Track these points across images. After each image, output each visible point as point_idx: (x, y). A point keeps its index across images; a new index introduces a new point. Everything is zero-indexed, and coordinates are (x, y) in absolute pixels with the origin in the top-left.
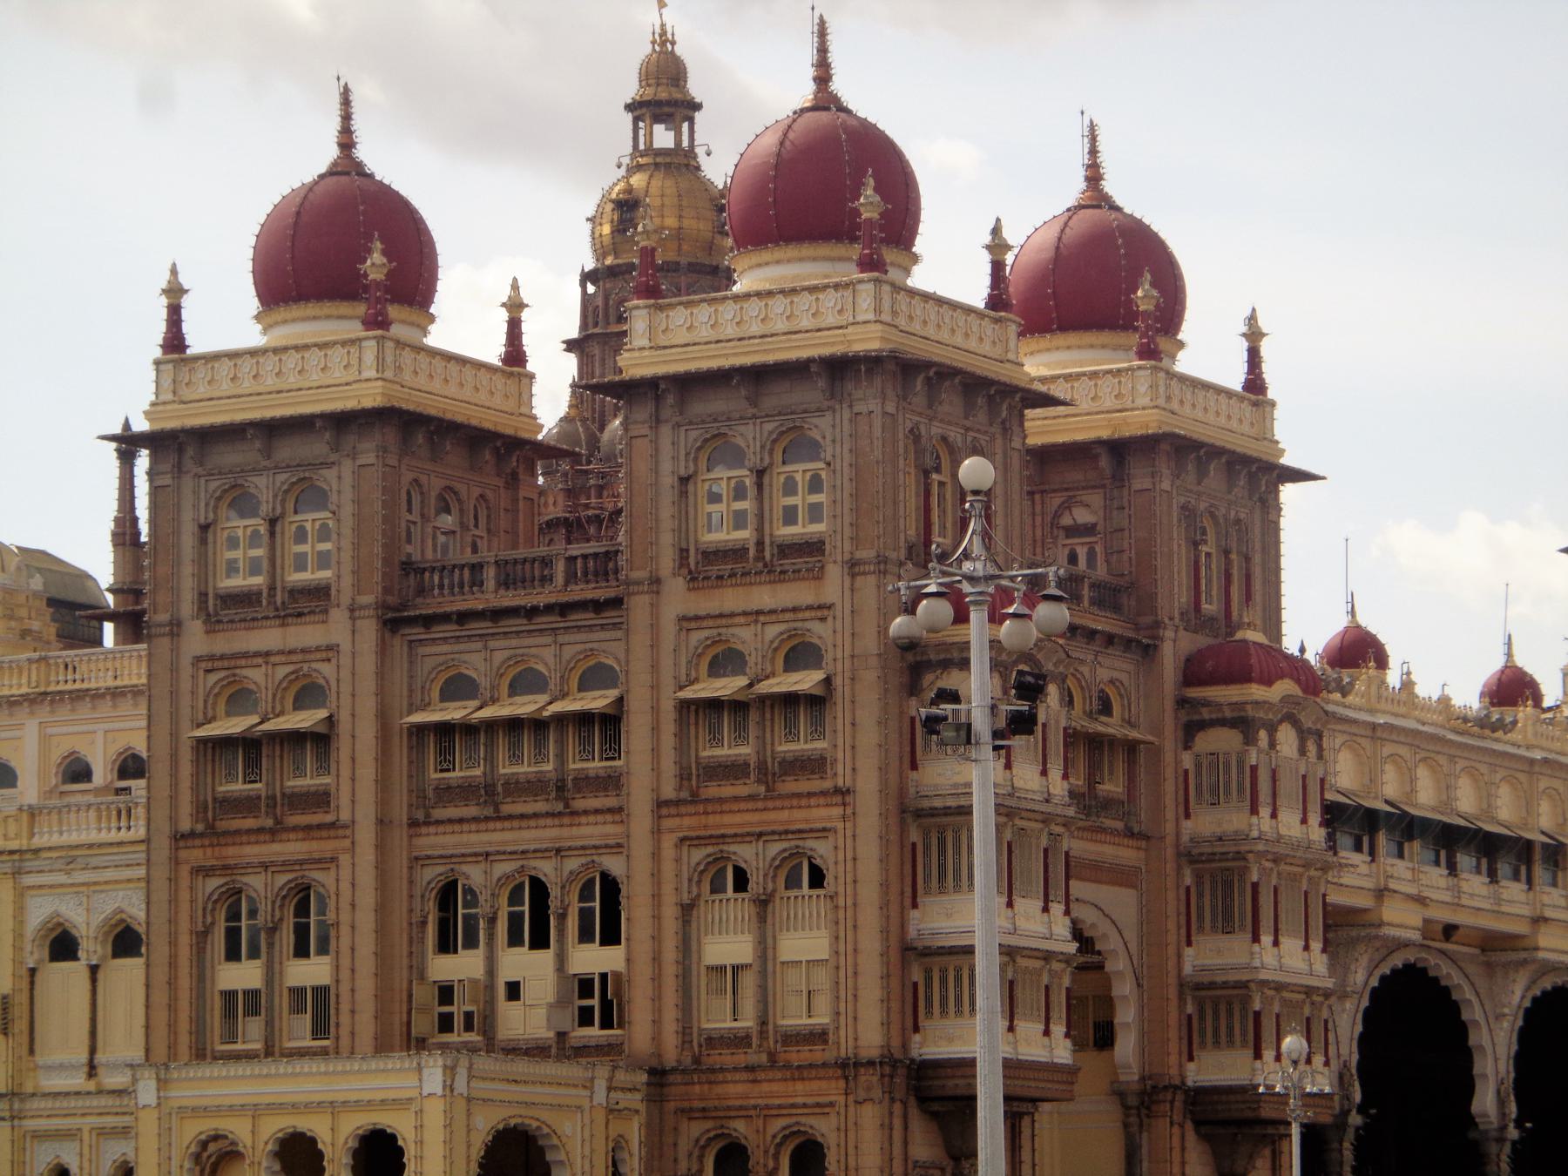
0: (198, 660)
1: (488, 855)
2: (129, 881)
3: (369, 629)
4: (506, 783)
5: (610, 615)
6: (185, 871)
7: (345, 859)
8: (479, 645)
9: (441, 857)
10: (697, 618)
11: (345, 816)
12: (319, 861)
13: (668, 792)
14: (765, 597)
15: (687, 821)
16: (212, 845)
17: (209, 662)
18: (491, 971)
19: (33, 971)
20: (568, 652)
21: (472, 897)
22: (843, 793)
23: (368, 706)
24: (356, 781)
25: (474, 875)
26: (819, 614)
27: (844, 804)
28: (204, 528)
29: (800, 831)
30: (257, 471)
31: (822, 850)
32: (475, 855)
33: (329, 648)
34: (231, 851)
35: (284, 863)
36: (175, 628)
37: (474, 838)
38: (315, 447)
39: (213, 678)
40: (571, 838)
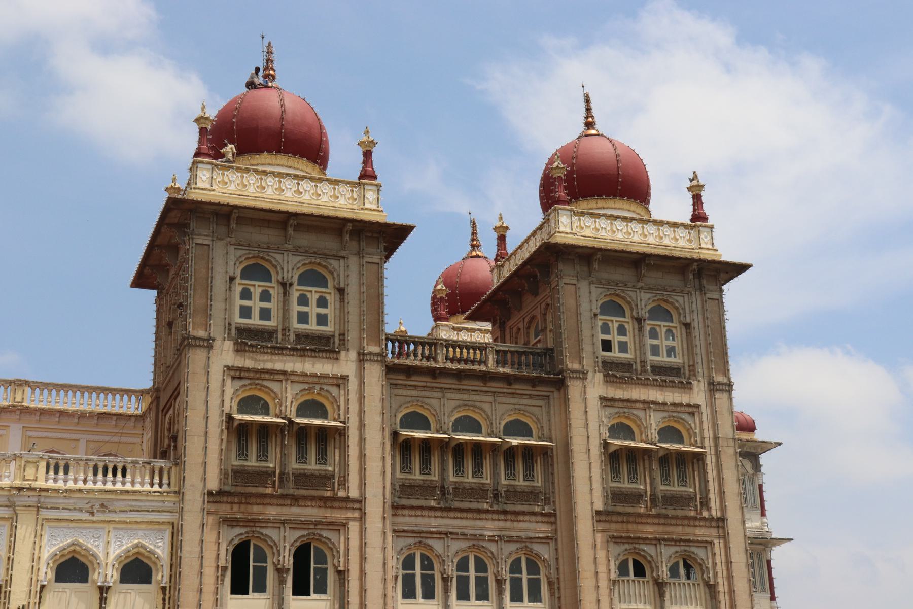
0: (229, 368)
2: (151, 523)
7: (354, 527)
8: (440, 395)
9: (413, 532)
11: (354, 493)
12: (332, 524)
13: (599, 506)
14: (655, 395)
15: (613, 526)
16: (240, 503)
17: (236, 373)
20: (501, 408)
21: (427, 564)
23: (374, 420)
24: (370, 469)
26: (691, 410)
27: (718, 527)
28: (232, 279)
29: (689, 541)
31: (700, 553)
32: (440, 533)
34: (255, 509)
35: (302, 523)
36: (208, 343)
38: (328, 243)
40: (514, 529)
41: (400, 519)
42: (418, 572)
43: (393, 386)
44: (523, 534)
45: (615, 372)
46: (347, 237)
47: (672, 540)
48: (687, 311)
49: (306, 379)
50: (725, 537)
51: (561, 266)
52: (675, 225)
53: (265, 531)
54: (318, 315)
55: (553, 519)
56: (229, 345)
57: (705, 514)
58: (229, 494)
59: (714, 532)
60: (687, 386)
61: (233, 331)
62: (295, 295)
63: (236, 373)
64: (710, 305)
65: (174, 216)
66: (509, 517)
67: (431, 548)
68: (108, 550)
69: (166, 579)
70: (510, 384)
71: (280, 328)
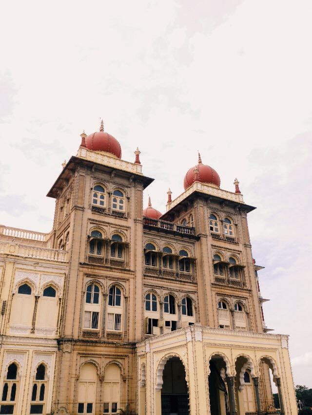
0: (90, 219)
1: (165, 287)
2: (57, 273)
3: (140, 227)
4: (164, 271)
5: (192, 241)
6: (81, 274)
9: (151, 285)
10: (215, 246)
11: (132, 269)
12: (124, 279)
17: (92, 221)
18: (162, 317)
19: (13, 294)
22: (250, 291)
25: (158, 291)
30: (108, 182)
31: (244, 302)
32: (159, 287)
33: (129, 228)
34: (97, 271)
35: (113, 278)
36: (83, 209)
37: (159, 282)
39: (92, 225)
41: (146, 280)
42: (151, 301)
43: (145, 233)
44: (187, 290)
45: (216, 237)
46: (131, 180)
47: (235, 296)
48: (236, 220)
49: (116, 227)
50: (252, 296)
51: (198, 201)
52: (232, 193)
53: (99, 280)
54: (120, 206)
55: (196, 285)
56: (90, 211)
57: (245, 288)
58: (88, 265)
59: (248, 294)
60: (237, 244)
61: (91, 207)
62: (112, 198)
63: (92, 221)
64: (243, 219)
65: (71, 167)
66: (182, 283)
67: (156, 292)
68: (39, 283)
69: (62, 295)
70: (182, 237)
71: (107, 209)
